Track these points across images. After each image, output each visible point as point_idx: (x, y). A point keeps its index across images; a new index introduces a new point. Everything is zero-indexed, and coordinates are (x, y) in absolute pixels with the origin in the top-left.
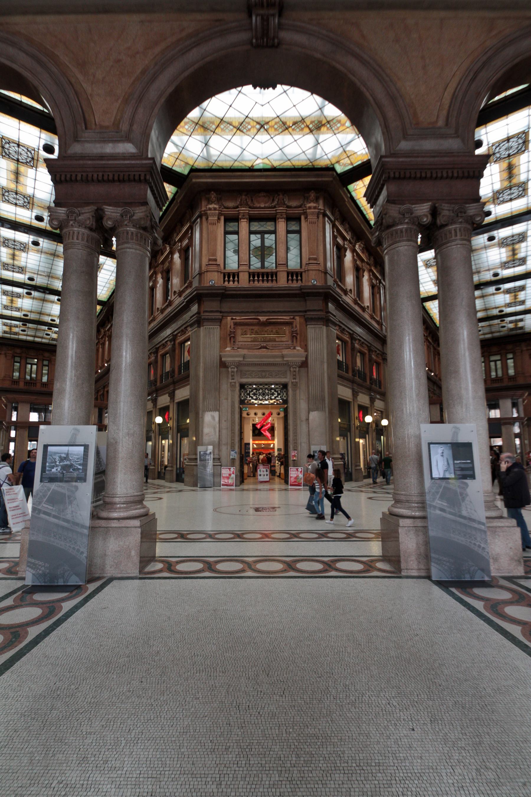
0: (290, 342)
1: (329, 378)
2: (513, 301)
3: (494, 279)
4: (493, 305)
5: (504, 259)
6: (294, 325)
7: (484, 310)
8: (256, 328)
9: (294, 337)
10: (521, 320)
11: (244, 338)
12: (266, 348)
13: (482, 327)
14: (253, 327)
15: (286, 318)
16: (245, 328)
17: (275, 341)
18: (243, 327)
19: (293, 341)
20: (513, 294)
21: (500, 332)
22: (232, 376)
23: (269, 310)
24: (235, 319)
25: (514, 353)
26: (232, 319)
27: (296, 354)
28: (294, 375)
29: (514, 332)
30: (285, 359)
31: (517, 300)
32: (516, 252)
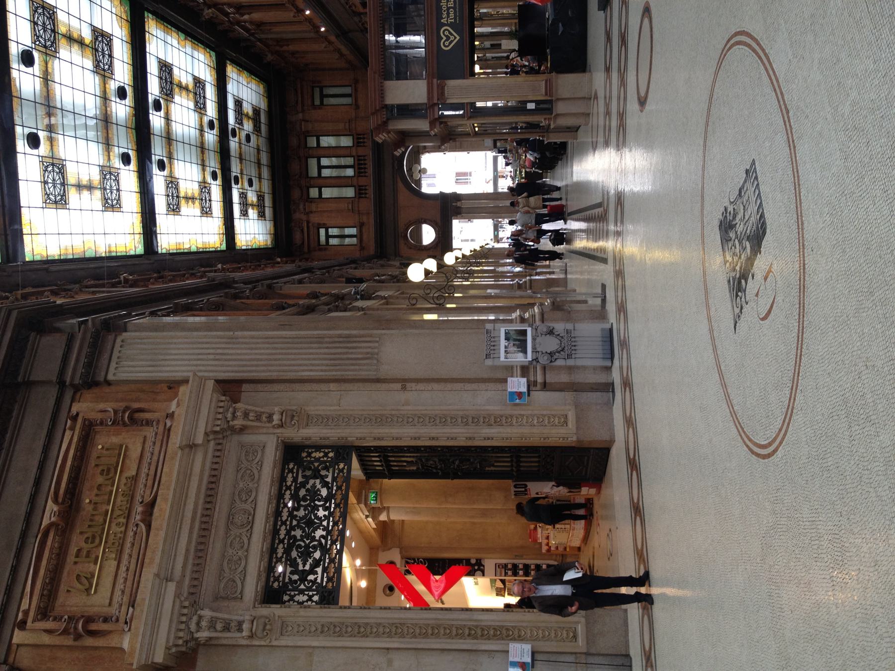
0: (149, 432)
1: (282, 327)
2: (191, 95)
3: (129, 100)
4: (194, 133)
5: (89, 64)
6: (99, 416)
7: (203, 153)
8: (77, 542)
9: (132, 419)
10: (238, 103)
11: (98, 588)
12: (152, 504)
13: (242, 173)
14: (73, 550)
15: (68, 441)
16: (67, 579)
17: (135, 478)
18: (63, 588)
19: (149, 423)
20: (177, 90)
21: (258, 150)
22: (227, 628)
23: (26, 499)
24: (26, 613)
25: (307, 134)
26: (22, 625)
27: (191, 415)
28: (258, 418)
29: (264, 128)
30: (199, 440)
31: (191, 86)
32: (75, 36)
